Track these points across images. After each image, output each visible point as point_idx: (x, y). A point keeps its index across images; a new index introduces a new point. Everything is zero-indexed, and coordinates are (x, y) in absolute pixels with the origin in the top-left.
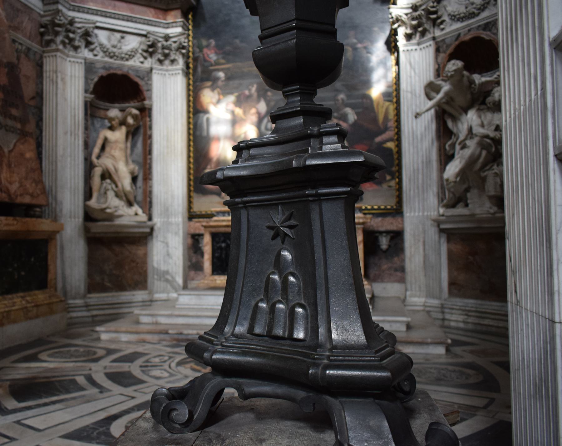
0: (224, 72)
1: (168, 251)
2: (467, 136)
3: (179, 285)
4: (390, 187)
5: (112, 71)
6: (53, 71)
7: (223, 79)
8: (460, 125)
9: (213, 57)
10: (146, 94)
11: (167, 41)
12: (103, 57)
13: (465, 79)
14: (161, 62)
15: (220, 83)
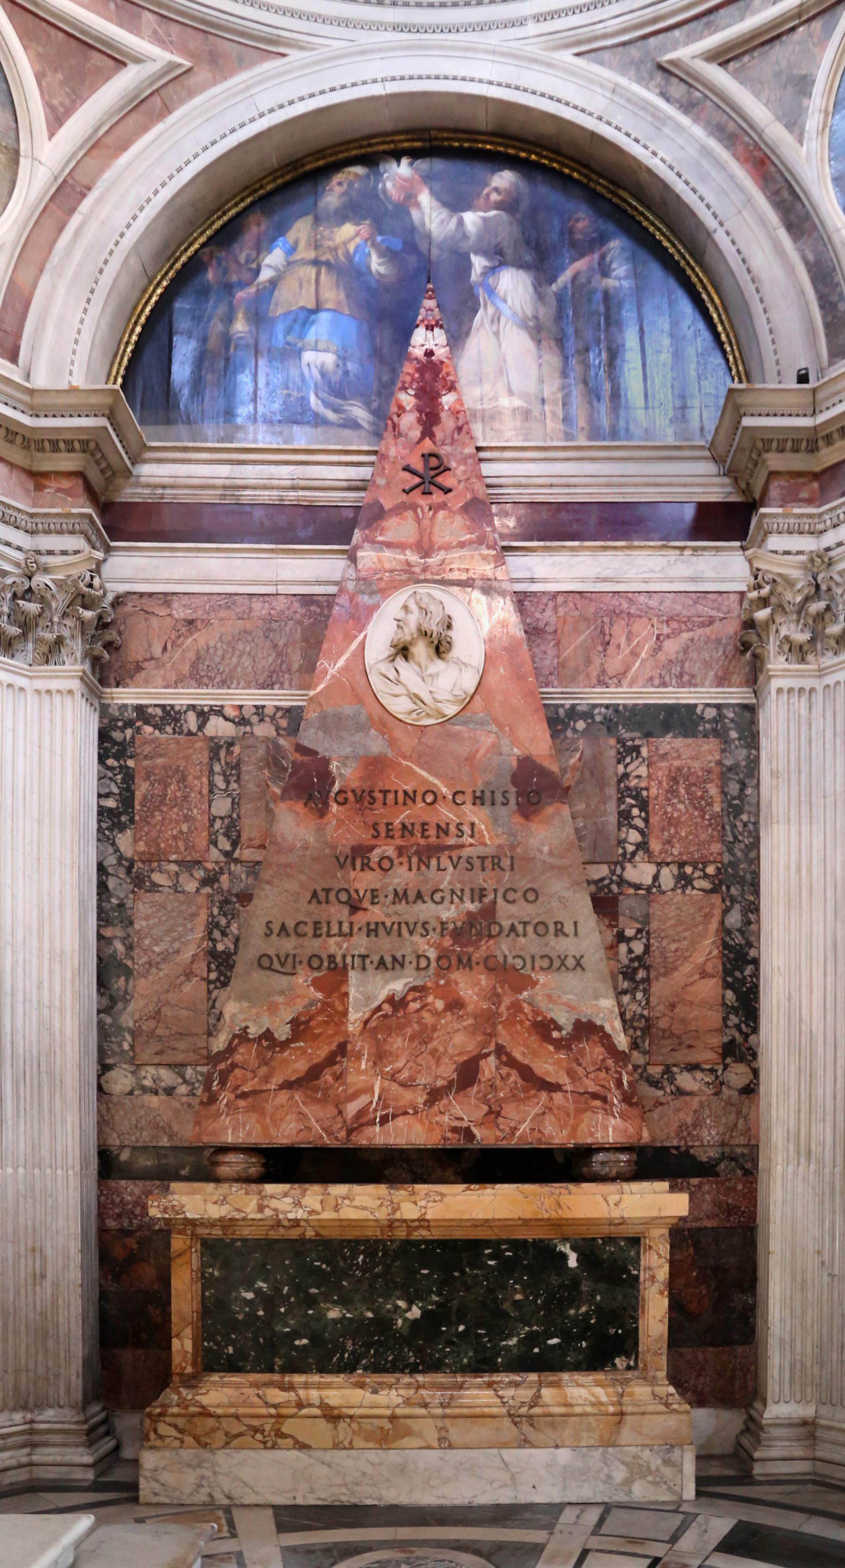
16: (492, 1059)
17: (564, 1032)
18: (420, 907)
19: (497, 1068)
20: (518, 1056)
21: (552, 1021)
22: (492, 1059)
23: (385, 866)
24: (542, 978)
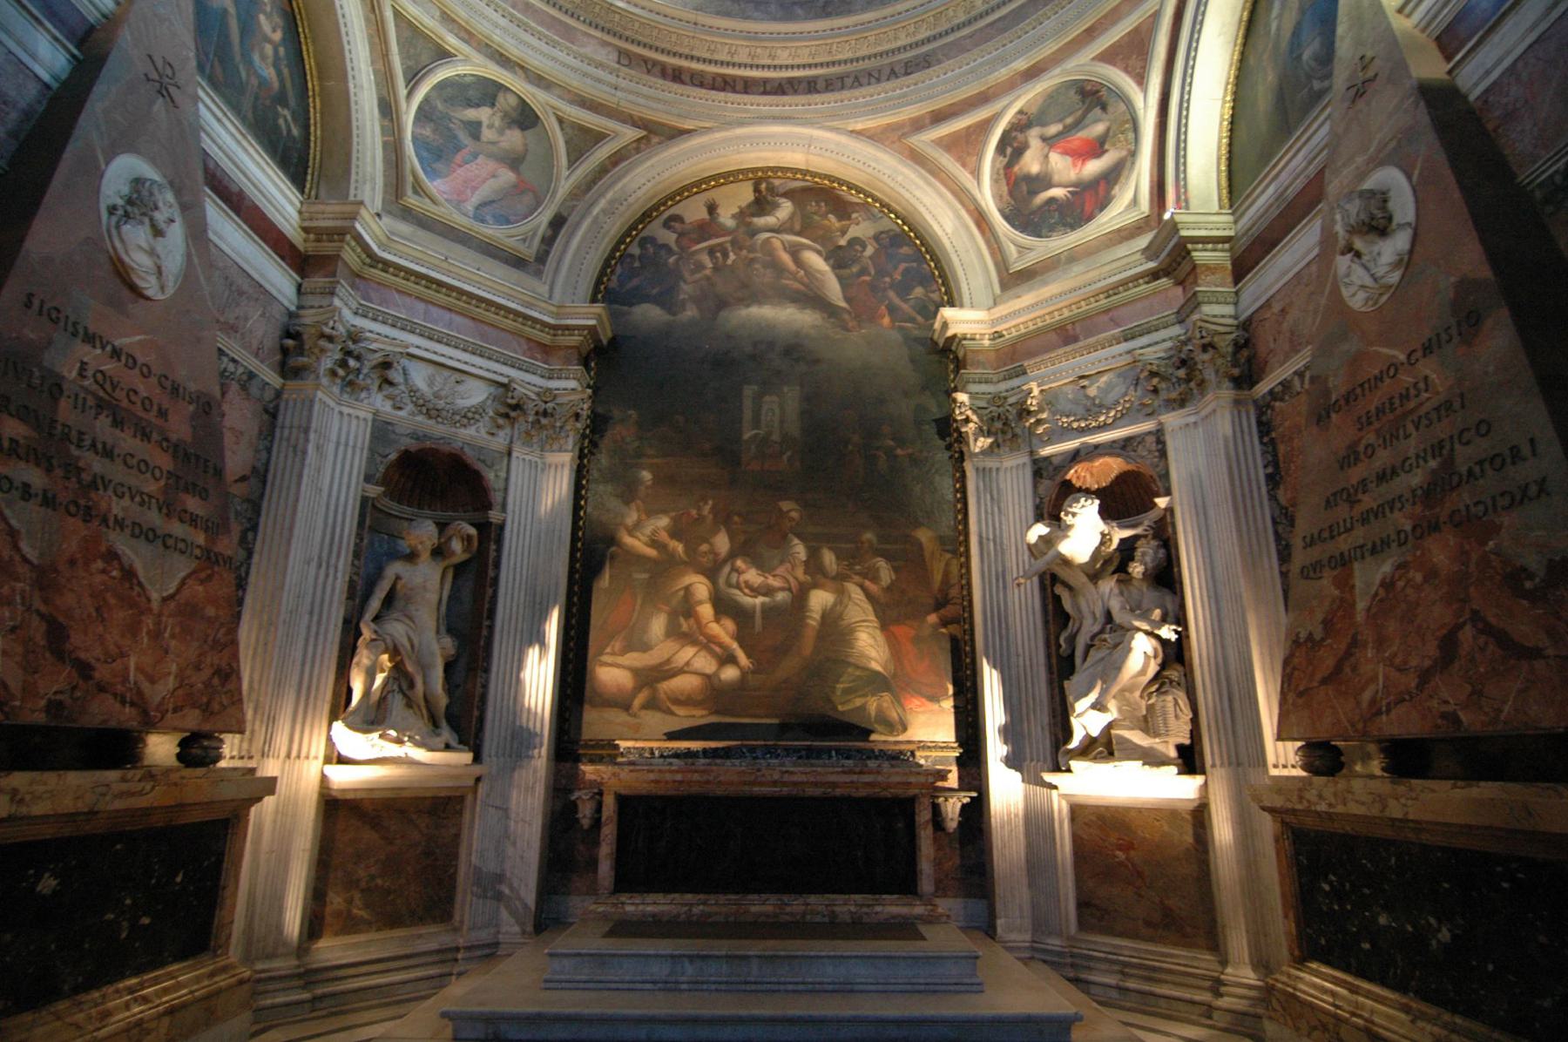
0: (652, 472)
1: (506, 828)
3: (526, 906)
5: (428, 444)
6: (299, 427)
7: (649, 483)
10: (497, 497)
12: (413, 414)
16: (1468, 628)
17: (1537, 580)
18: (1397, 480)
19: (1474, 638)
20: (1492, 620)
21: (1523, 569)
22: (1468, 628)
23: (1371, 451)
24: (1506, 520)
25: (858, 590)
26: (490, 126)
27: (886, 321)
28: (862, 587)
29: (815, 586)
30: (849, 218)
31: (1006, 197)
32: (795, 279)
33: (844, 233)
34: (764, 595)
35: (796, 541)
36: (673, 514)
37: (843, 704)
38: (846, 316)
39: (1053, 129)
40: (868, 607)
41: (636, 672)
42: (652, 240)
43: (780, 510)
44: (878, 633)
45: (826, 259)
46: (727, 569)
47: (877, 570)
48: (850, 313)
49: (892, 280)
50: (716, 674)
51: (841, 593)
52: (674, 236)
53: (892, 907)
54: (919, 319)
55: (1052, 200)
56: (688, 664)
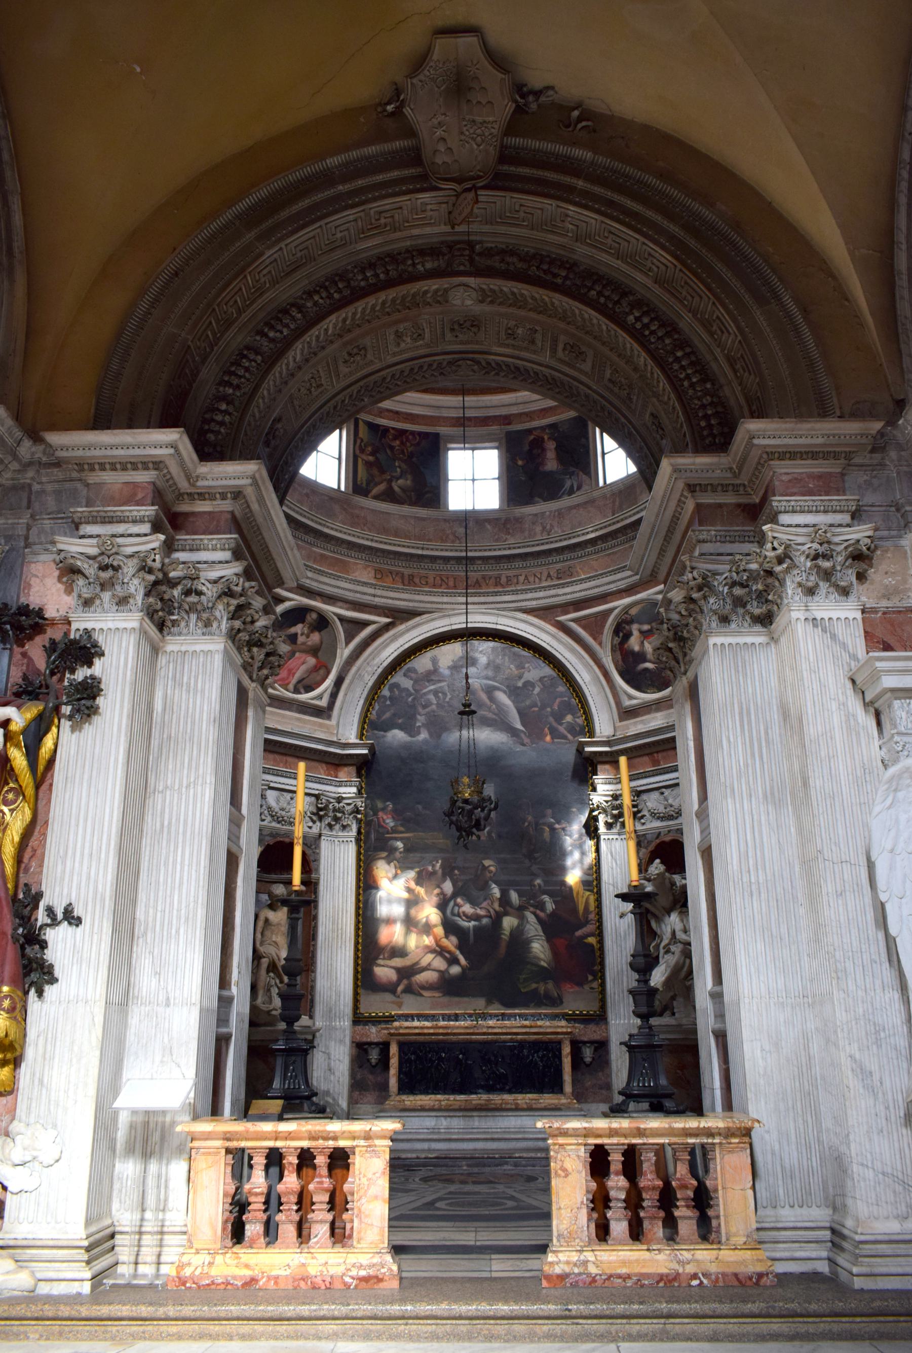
2: (671, 939)
4: (592, 988)
8: (663, 926)
9: (390, 823)
11: (339, 803)
13: (667, 881)
14: (330, 826)
15: (397, 855)
25: (533, 916)
26: (302, 634)
27: (548, 738)
28: (535, 914)
29: (506, 914)
30: (523, 668)
31: (620, 662)
32: (490, 711)
33: (520, 677)
34: (475, 920)
35: (494, 886)
36: (417, 870)
37: (524, 988)
38: (523, 735)
39: (646, 627)
40: (539, 928)
41: (399, 970)
42: (396, 686)
43: (484, 866)
44: (545, 944)
45: (509, 697)
46: (452, 903)
47: (544, 903)
48: (525, 734)
49: (552, 710)
50: (447, 970)
51: (522, 918)
52: (412, 682)
53: (548, 1099)
54: (569, 736)
55: (646, 669)
56: (429, 964)
